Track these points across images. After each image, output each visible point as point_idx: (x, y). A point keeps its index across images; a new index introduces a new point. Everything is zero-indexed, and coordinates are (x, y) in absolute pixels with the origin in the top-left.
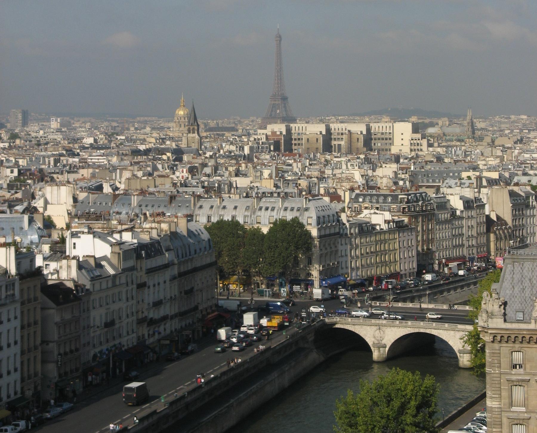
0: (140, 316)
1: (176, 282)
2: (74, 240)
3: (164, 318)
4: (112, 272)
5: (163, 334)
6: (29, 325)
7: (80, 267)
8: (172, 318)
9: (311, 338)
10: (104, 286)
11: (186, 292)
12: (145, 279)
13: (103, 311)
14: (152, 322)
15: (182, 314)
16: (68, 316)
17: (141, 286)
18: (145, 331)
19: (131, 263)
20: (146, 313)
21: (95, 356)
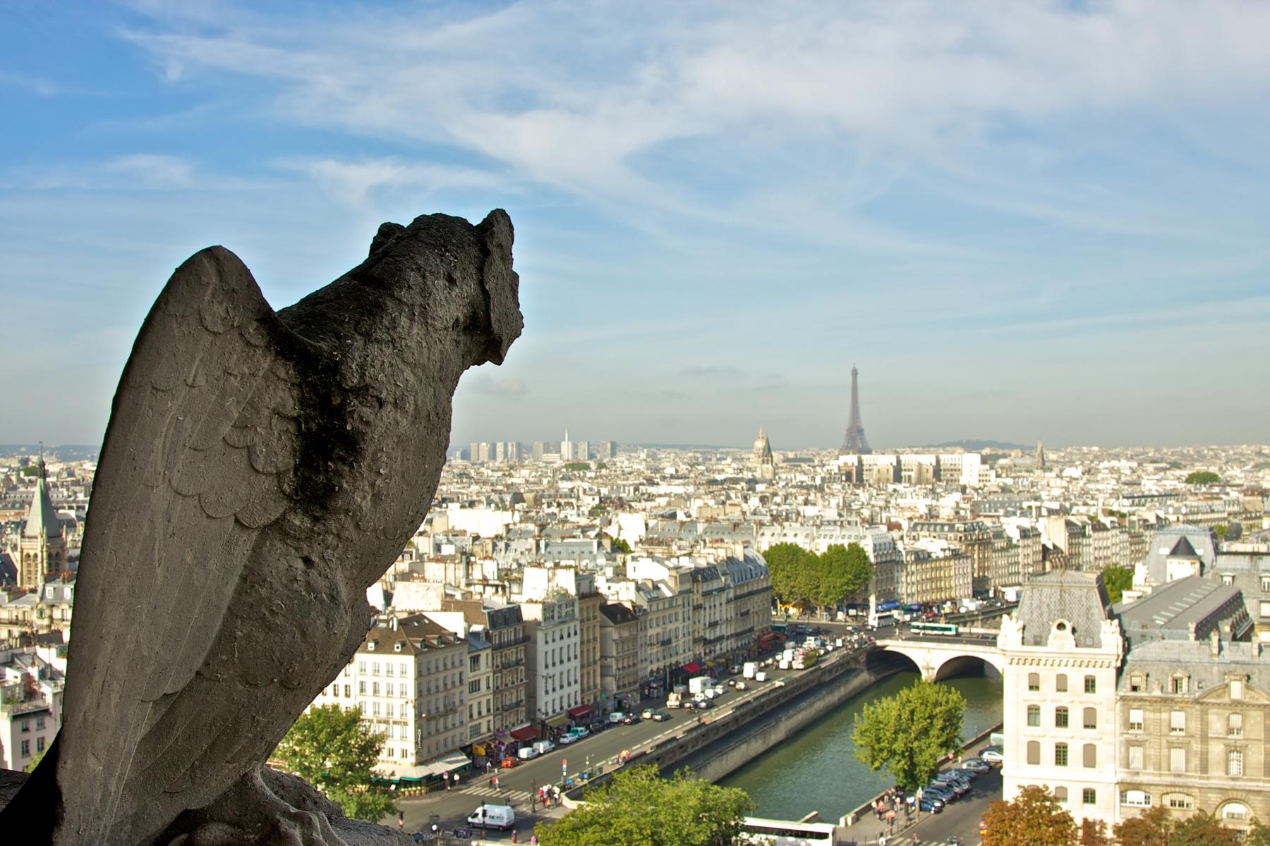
1: (732, 605)
2: (635, 563)
3: (720, 638)
4: (668, 594)
5: (718, 652)
6: (589, 641)
7: (638, 589)
8: (728, 638)
9: (862, 659)
10: (661, 607)
11: (742, 615)
12: (701, 601)
14: (706, 642)
15: (737, 635)
16: (626, 634)
17: (698, 608)
18: (700, 650)
19: (687, 586)
20: (702, 633)
21: (652, 672)
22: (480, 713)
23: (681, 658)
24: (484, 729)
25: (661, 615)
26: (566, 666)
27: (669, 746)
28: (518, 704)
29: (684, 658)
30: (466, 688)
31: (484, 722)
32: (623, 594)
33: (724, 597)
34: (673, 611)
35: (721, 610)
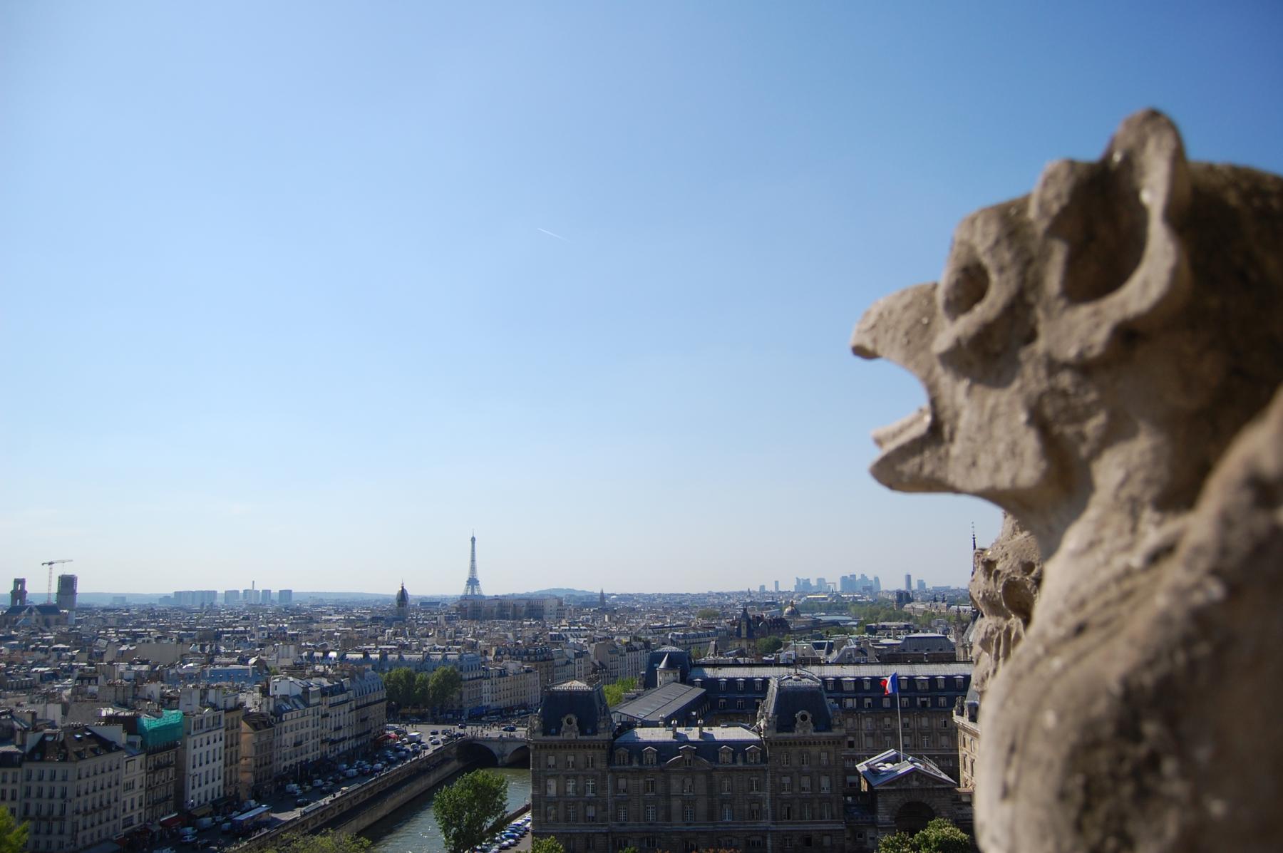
14: (333, 742)
15: (358, 736)
16: (263, 738)
17: (327, 715)
18: (326, 748)
22: (132, 807)
24: (136, 820)
25: (293, 722)
26: (212, 765)
28: (167, 798)
29: (311, 756)
30: (121, 787)
31: (136, 815)
33: (347, 707)
34: (304, 719)
35: (344, 716)
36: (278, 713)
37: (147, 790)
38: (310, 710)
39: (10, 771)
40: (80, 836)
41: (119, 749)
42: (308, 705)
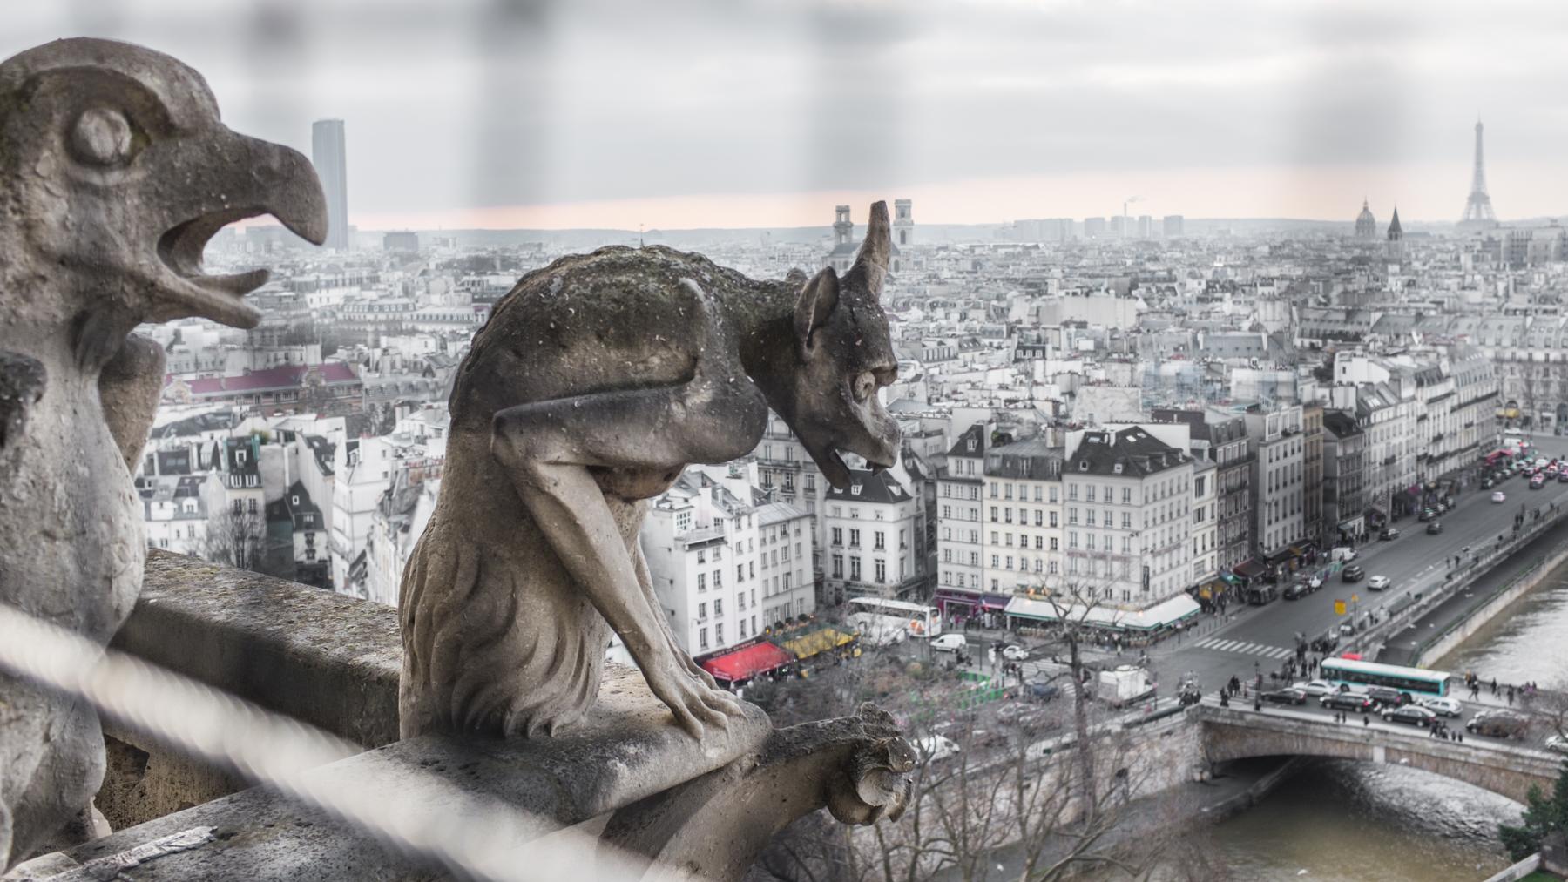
0: (1421, 452)
1: (1456, 414)
3: (1444, 456)
13: (1383, 445)
14: (1431, 461)
16: (1350, 451)
17: (1422, 418)
18: (1423, 468)
23: (1404, 480)
24: (1208, 567)
25: (1384, 427)
26: (1291, 489)
27: (1434, 594)
28: (1241, 537)
29: (1406, 479)
30: (1191, 517)
31: (1207, 557)
32: (1344, 400)
34: (1396, 422)
36: (1364, 411)
37: (1219, 524)
38: (1403, 409)
39: (1046, 486)
40: (1152, 582)
41: (1188, 460)
42: (1401, 401)
